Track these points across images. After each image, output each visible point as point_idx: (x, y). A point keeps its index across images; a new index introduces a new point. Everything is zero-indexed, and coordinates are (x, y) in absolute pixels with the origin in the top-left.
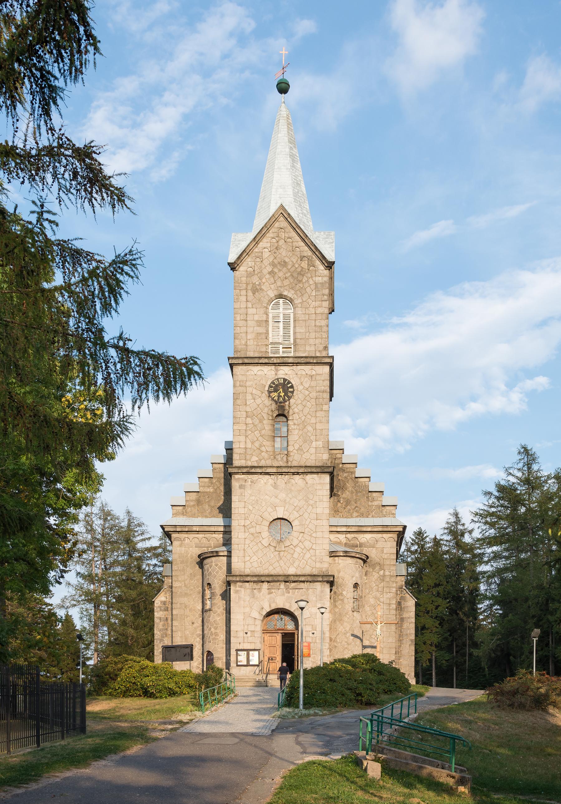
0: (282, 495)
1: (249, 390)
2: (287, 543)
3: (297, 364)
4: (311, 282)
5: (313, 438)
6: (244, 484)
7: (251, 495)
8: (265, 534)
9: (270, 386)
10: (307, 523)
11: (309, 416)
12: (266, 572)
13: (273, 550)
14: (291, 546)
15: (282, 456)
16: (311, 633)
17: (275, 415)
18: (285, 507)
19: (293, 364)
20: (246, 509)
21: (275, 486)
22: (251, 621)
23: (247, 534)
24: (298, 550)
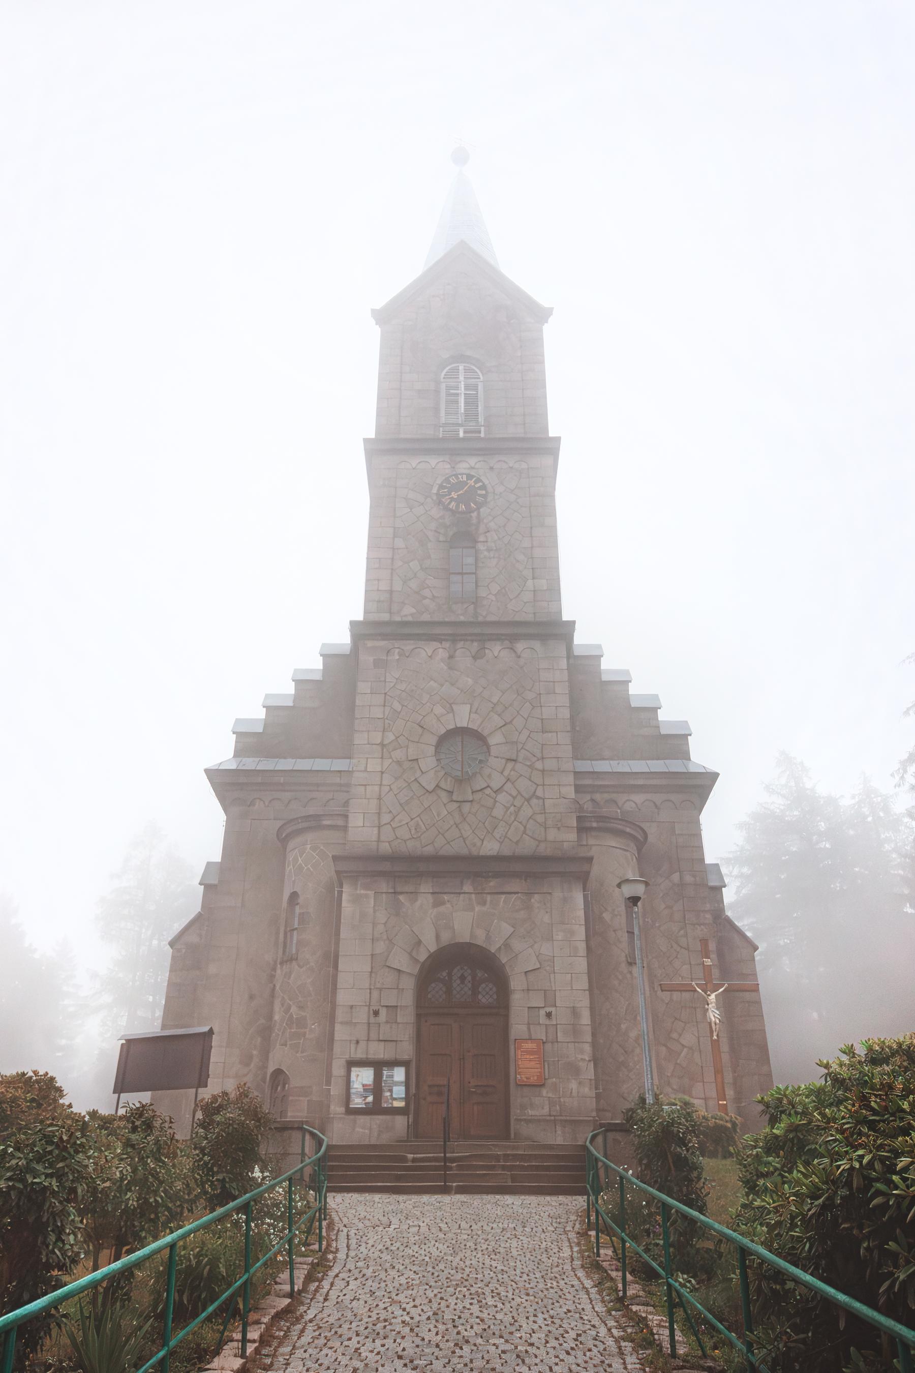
2: (479, 783)
6: (385, 658)
8: (428, 763)
9: (441, 487)
10: (523, 738)
12: (429, 850)
13: (445, 800)
14: (488, 791)
15: (465, 606)
16: (542, 1012)
17: (451, 533)
18: (471, 705)
20: (387, 709)
23: (387, 762)
24: (502, 798)
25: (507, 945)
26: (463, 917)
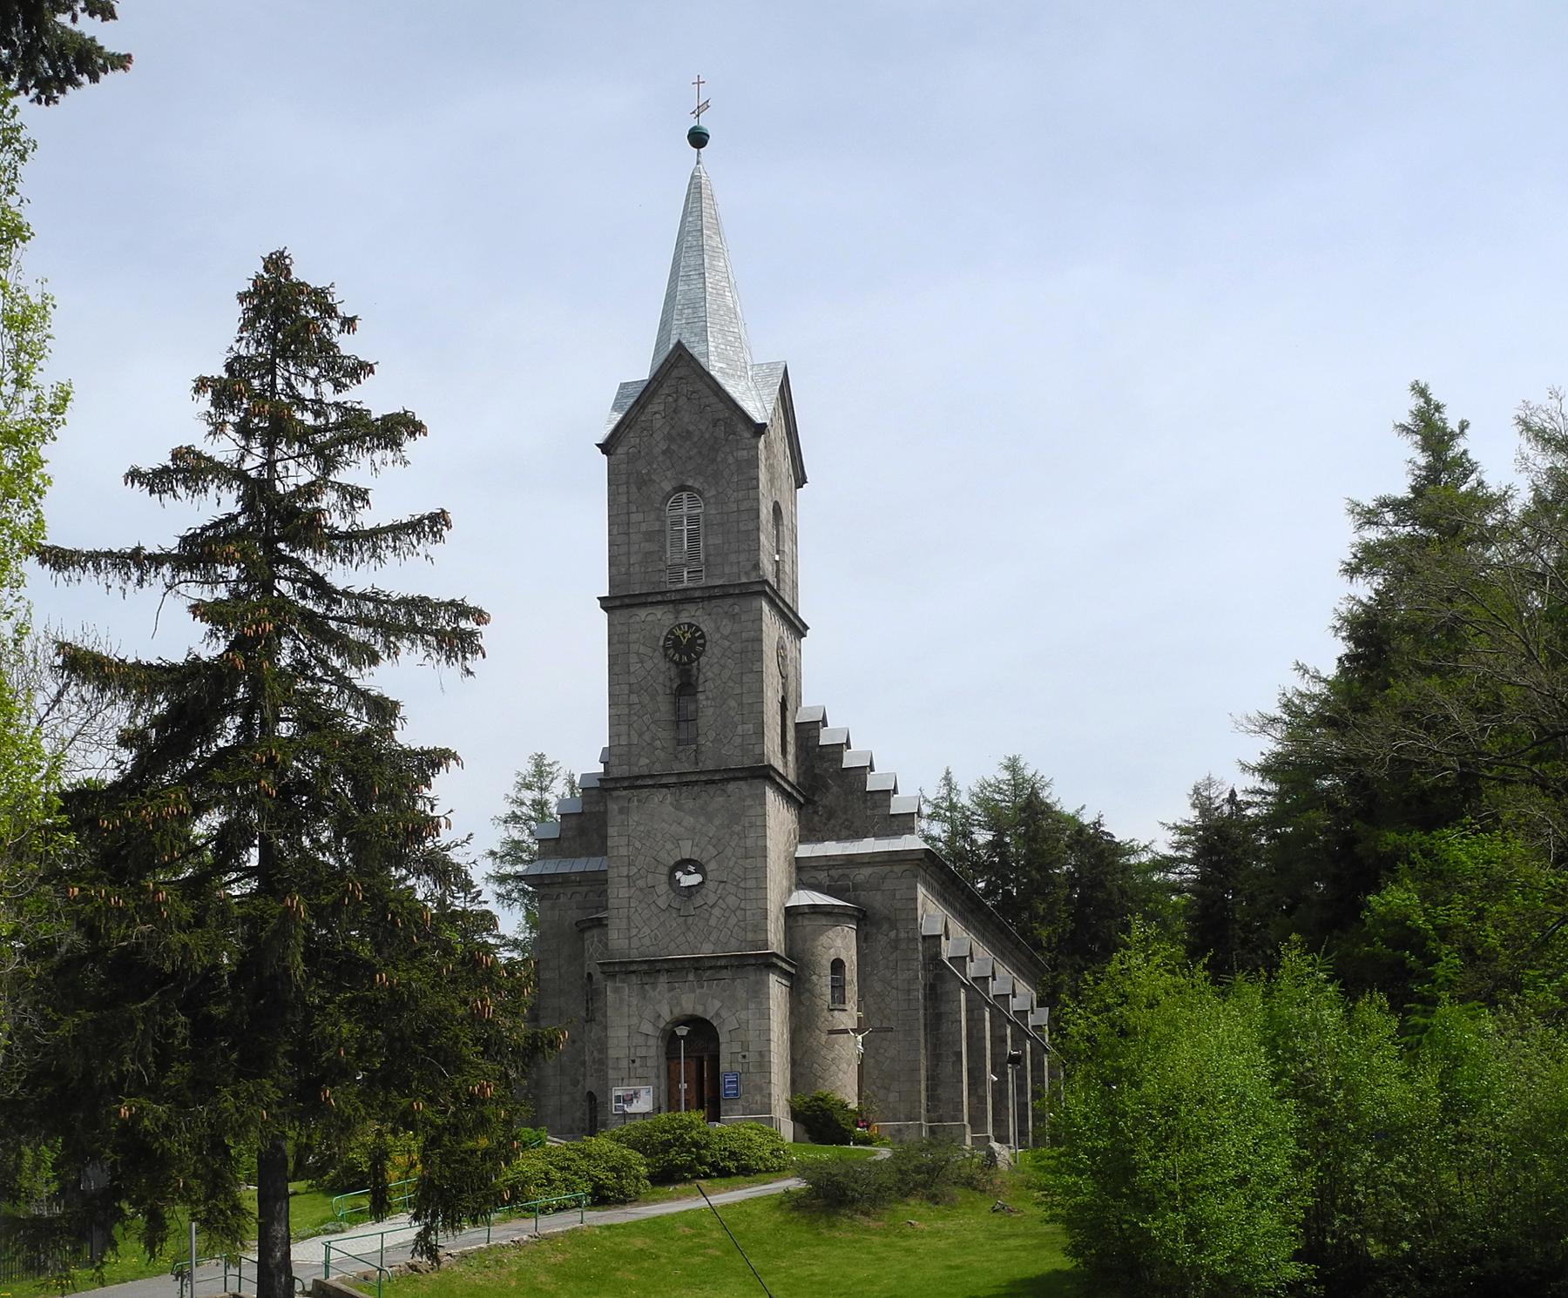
0: (689, 820)
1: (634, 647)
3: (710, 598)
4: (731, 459)
5: (737, 718)
7: (638, 824)
9: (667, 639)
10: (731, 864)
11: (731, 684)
19: (703, 599)
21: (678, 807)
22: (640, 1040)
24: (716, 912)
25: (717, 1014)
26: (691, 1000)
